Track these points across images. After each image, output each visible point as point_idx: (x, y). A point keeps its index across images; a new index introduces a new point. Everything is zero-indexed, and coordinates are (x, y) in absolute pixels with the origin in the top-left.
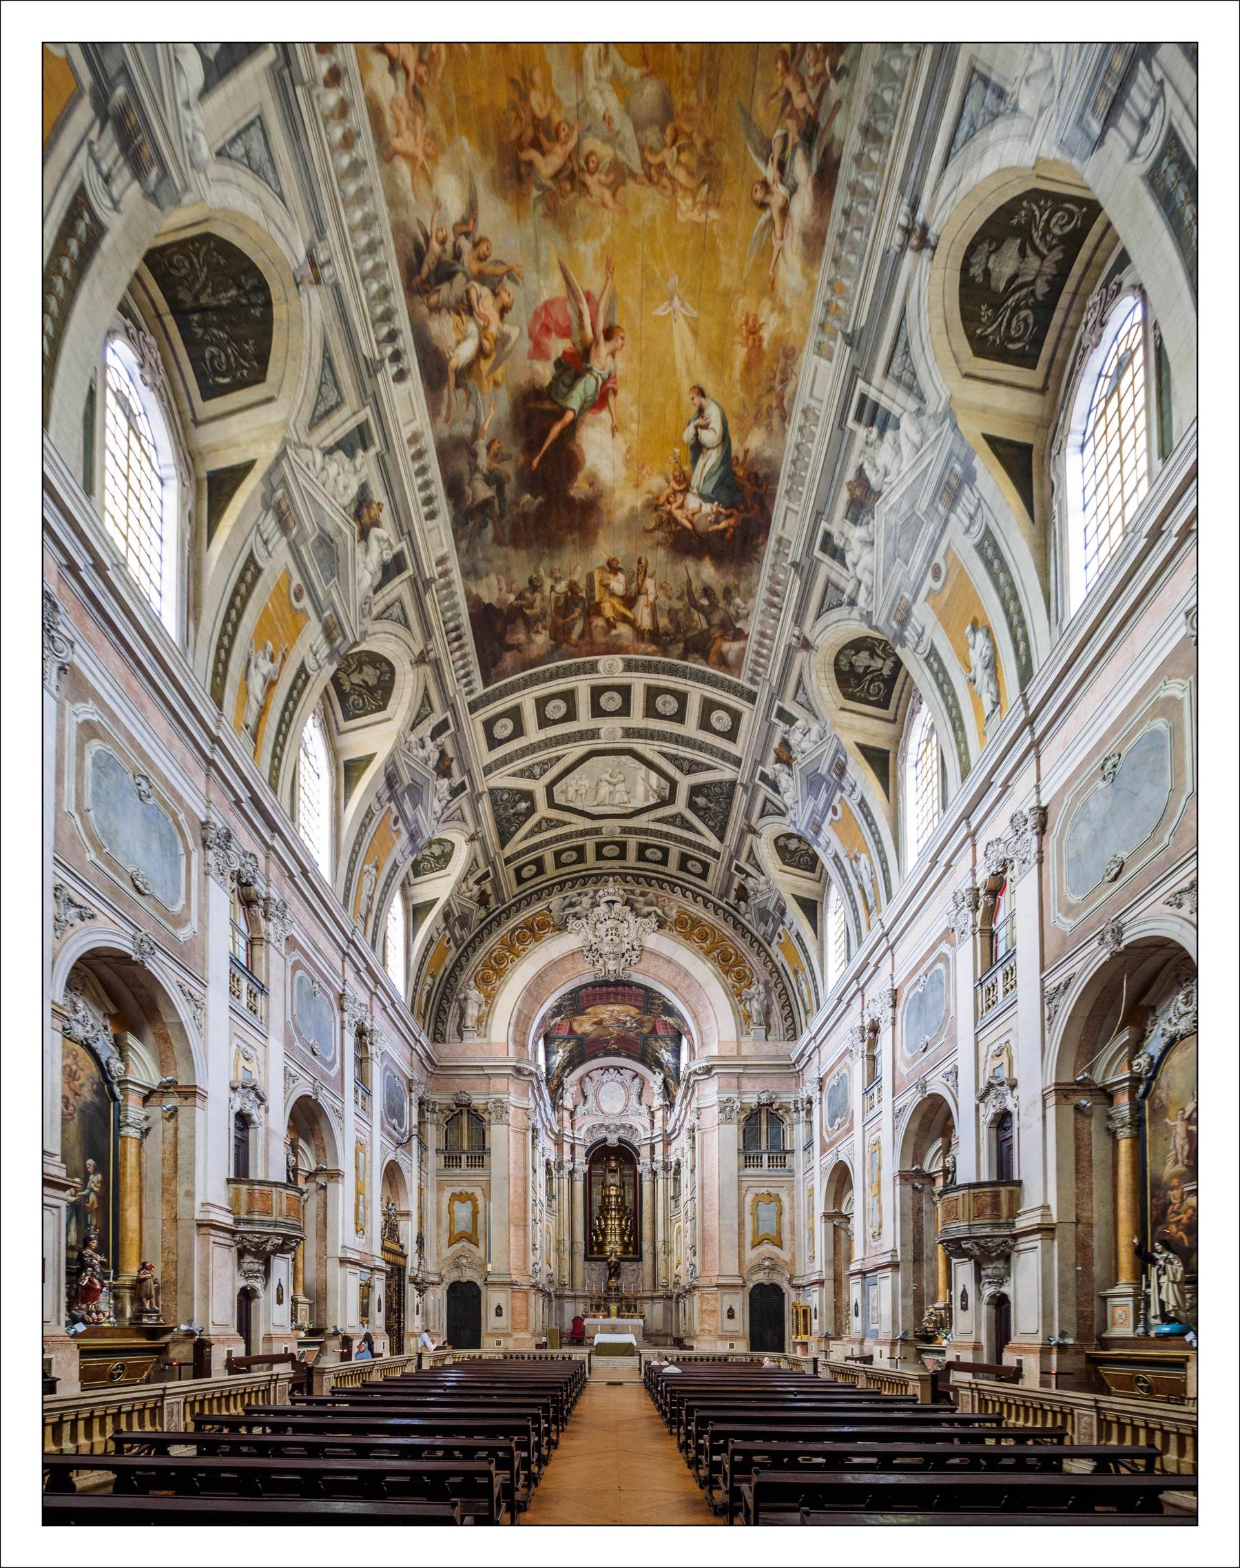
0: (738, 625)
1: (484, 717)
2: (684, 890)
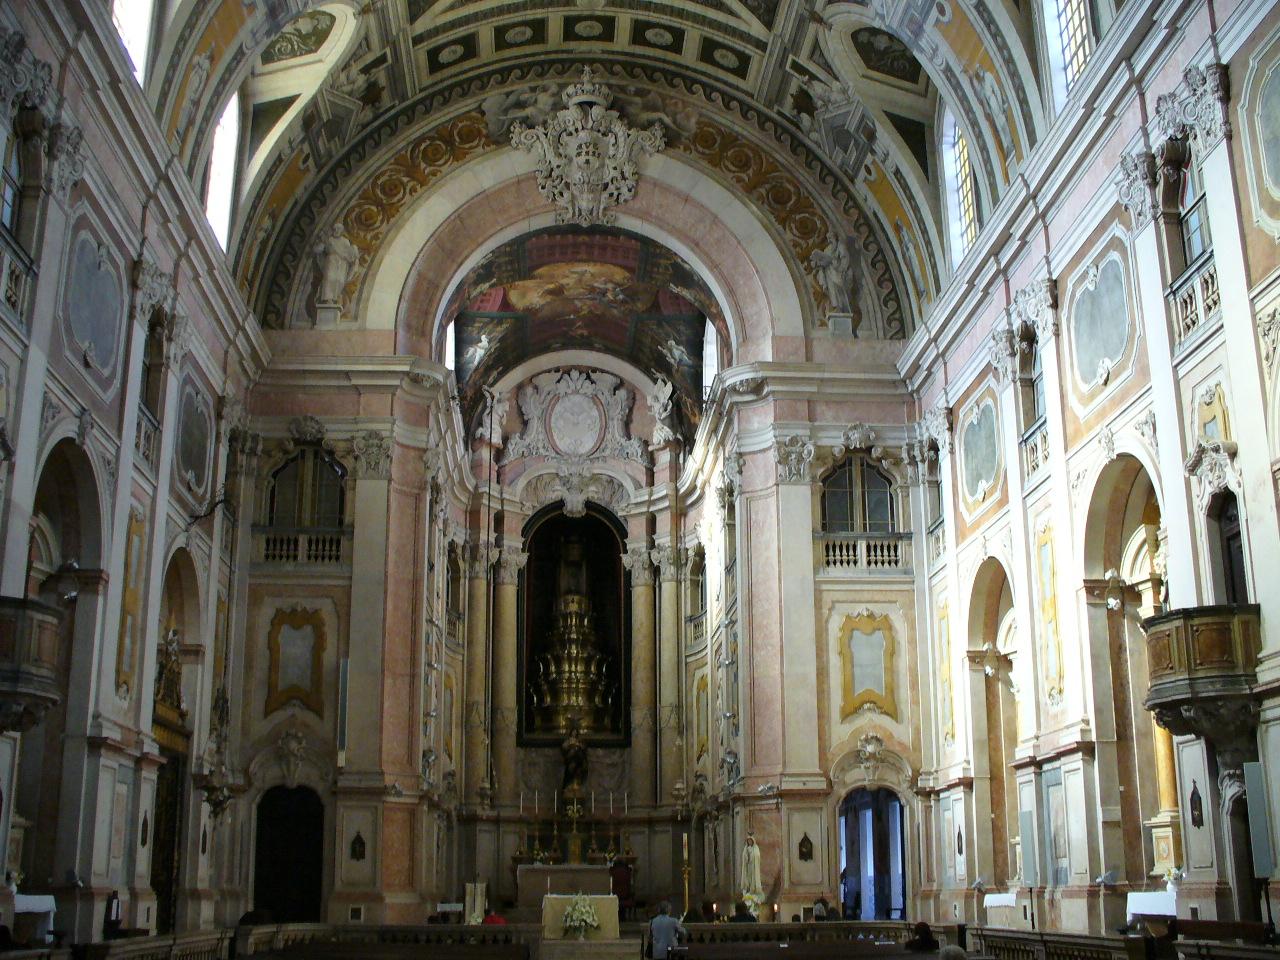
2: (709, 90)
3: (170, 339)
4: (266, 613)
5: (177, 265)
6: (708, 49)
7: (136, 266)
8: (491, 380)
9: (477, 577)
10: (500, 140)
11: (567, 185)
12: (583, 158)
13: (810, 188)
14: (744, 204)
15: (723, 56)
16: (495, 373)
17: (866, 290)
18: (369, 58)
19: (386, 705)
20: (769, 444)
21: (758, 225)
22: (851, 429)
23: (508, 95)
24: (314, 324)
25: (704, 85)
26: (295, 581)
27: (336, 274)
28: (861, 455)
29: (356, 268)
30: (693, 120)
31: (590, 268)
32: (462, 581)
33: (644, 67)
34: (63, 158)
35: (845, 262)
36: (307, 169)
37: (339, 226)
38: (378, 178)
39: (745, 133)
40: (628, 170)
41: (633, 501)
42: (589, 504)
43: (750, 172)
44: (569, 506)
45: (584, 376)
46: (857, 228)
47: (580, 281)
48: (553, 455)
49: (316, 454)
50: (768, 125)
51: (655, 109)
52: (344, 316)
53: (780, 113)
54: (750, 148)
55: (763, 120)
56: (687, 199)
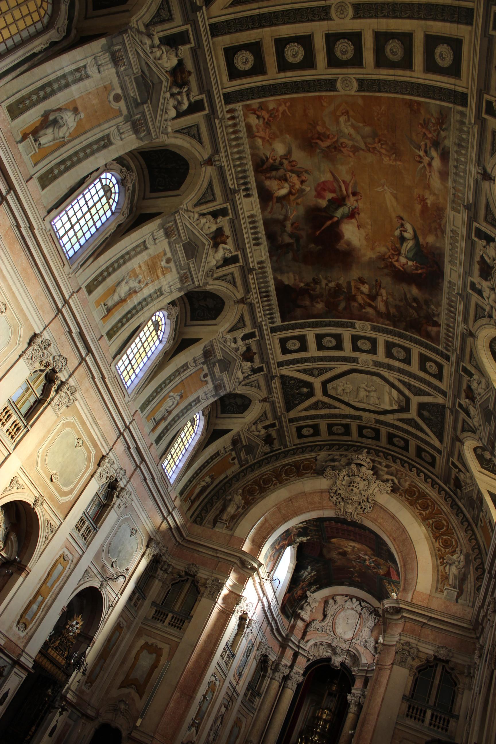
0: (435, 319)
1: (280, 336)
2: (419, 472)
3: (118, 497)
4: (141, 642)
5: (135, 470)
6: (419, 451)
7: (103, 457)
8: (312, 589)
9: (274, 679)
10: (320, 472)
11: (342, 498)
12: (351, 488)
13: (455, 526)
14: (420, 526)
15: (425, 456)
16: (314, 588)
17: (469, 580)
18: (268, 423)
19: (171, 705)
20: (395, 643)
21: (423, 536)
22: (439, 647)
23: (330, 455)
24: (214, 527)
25: (418, 469)
26: (159, 632)
27: (231, 510)
28: (444, 664)
29: (240, 509)
30: (408, 483)
31: (357, 545)
32: (267, 678)
33: (393, 456)
34: (63, 394)
35: (462, 564)
36: (234, 464)
37: (240, 491)
38: (263, 476)
39: (430, 494)
40: (371, 498)
41: (360, 668)
42: (342, 664)
43: (427, 512)
44: (332, 662)
45: (358, 602)
46: (473, 550)
47: (353, 551)
48: (332, 634)
49: (193, 581)
50: (443, 492)
51: (392, 474)
52: (227, 527)
53: (449, 488)
54: (432, 502)
55: (441, 489)
56: (393, 517)
